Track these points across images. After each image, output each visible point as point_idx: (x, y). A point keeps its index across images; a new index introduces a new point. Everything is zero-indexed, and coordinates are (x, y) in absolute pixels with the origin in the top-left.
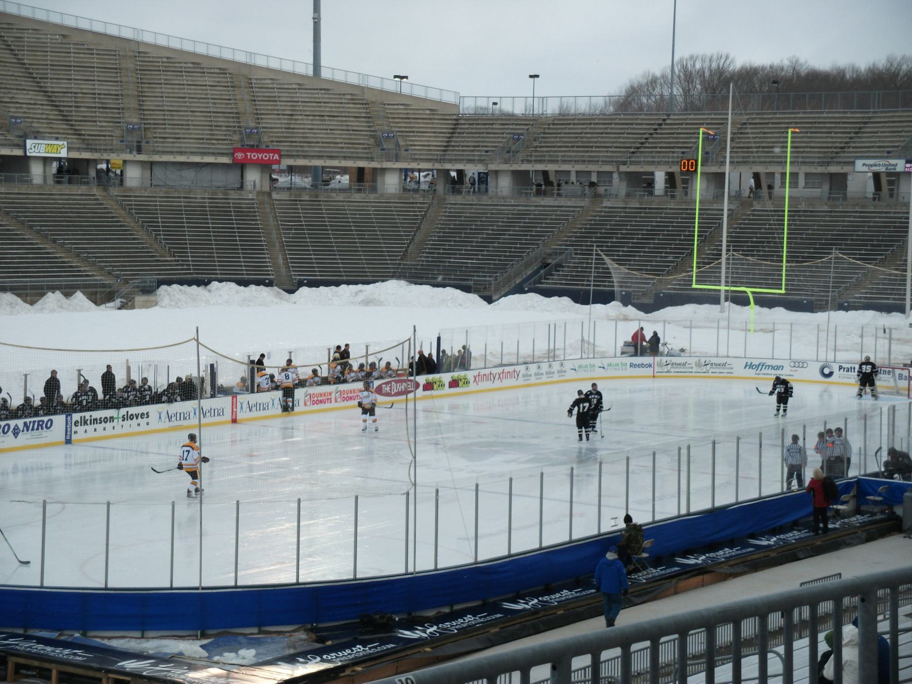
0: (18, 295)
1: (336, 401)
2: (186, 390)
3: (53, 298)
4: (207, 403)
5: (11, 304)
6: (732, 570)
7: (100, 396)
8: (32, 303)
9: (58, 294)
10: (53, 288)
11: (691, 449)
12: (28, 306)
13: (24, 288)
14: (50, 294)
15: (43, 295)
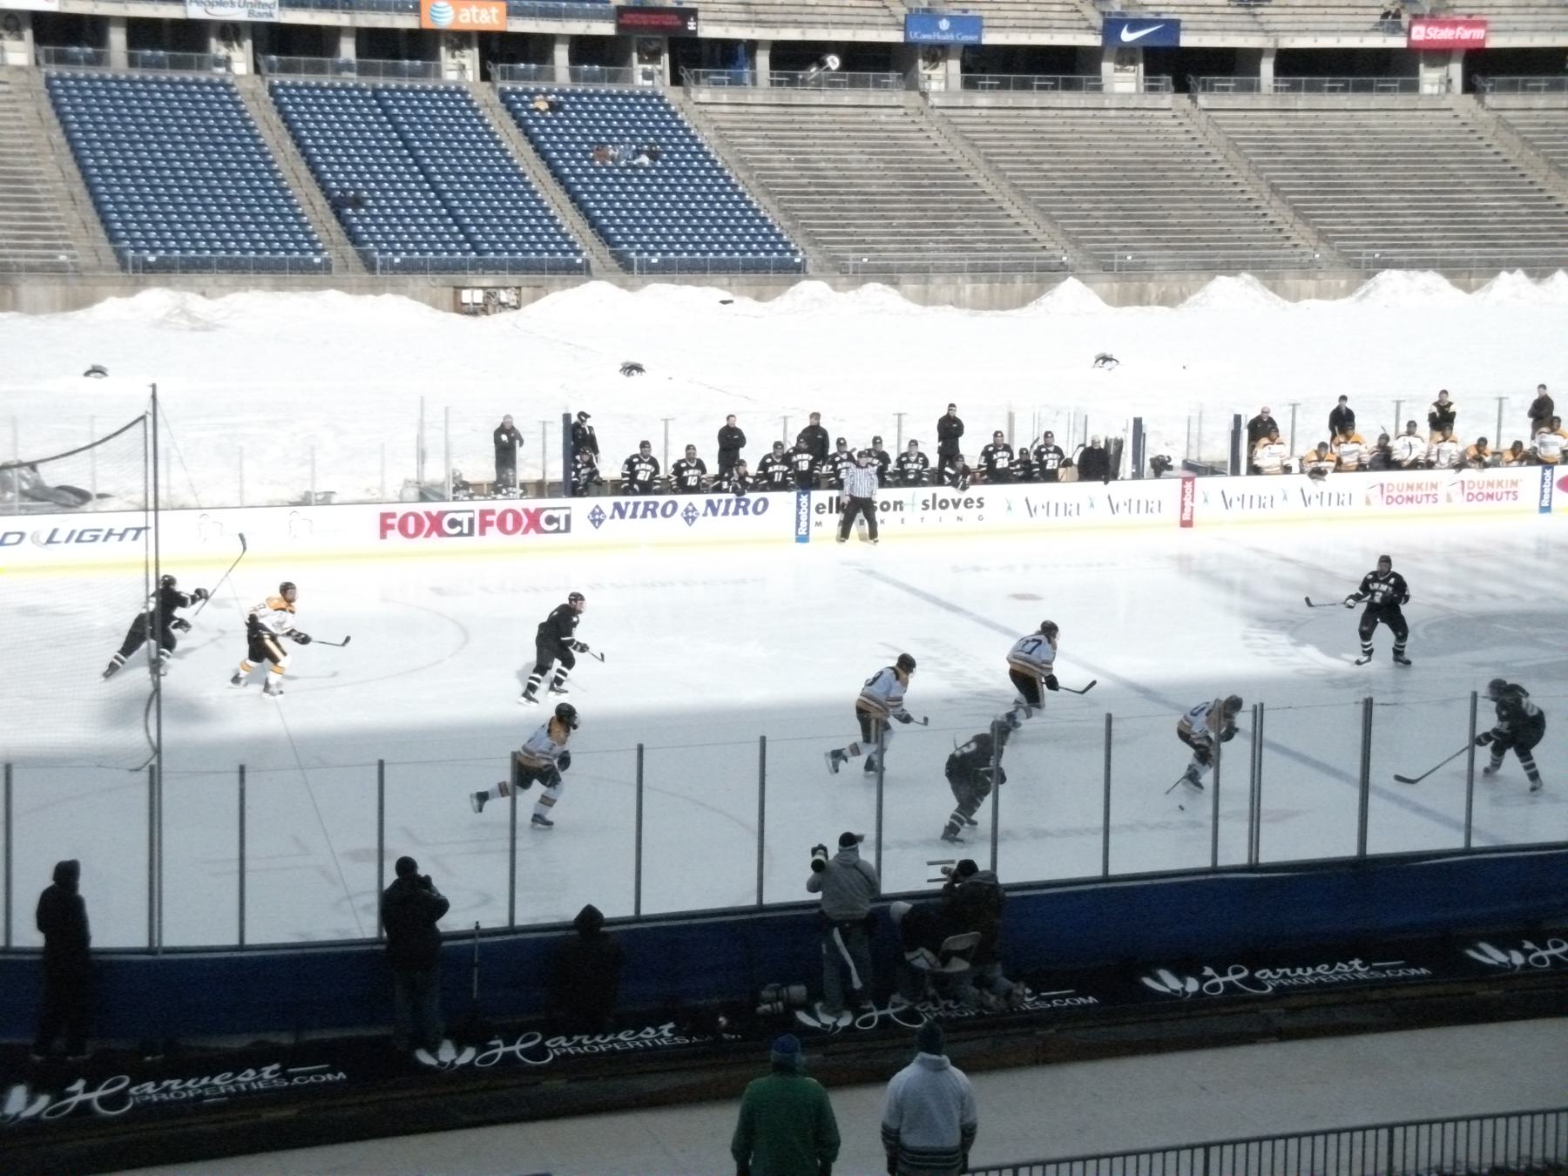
0: (1449, 275)
1: (1449, 499)
2: (1098, 464)
3: (1511, 283)
4: (1122, 488)
5: (1427, 290)
6: (1287, 1022)
7: (934, 461)
8: (1468, 289)
9: (1520, 275)
10: (1511, 265)
11: (386, 768)
12: (1460, 293)
13: (1456, 264)
14: (1504, 275)
15: (1496, 273)
